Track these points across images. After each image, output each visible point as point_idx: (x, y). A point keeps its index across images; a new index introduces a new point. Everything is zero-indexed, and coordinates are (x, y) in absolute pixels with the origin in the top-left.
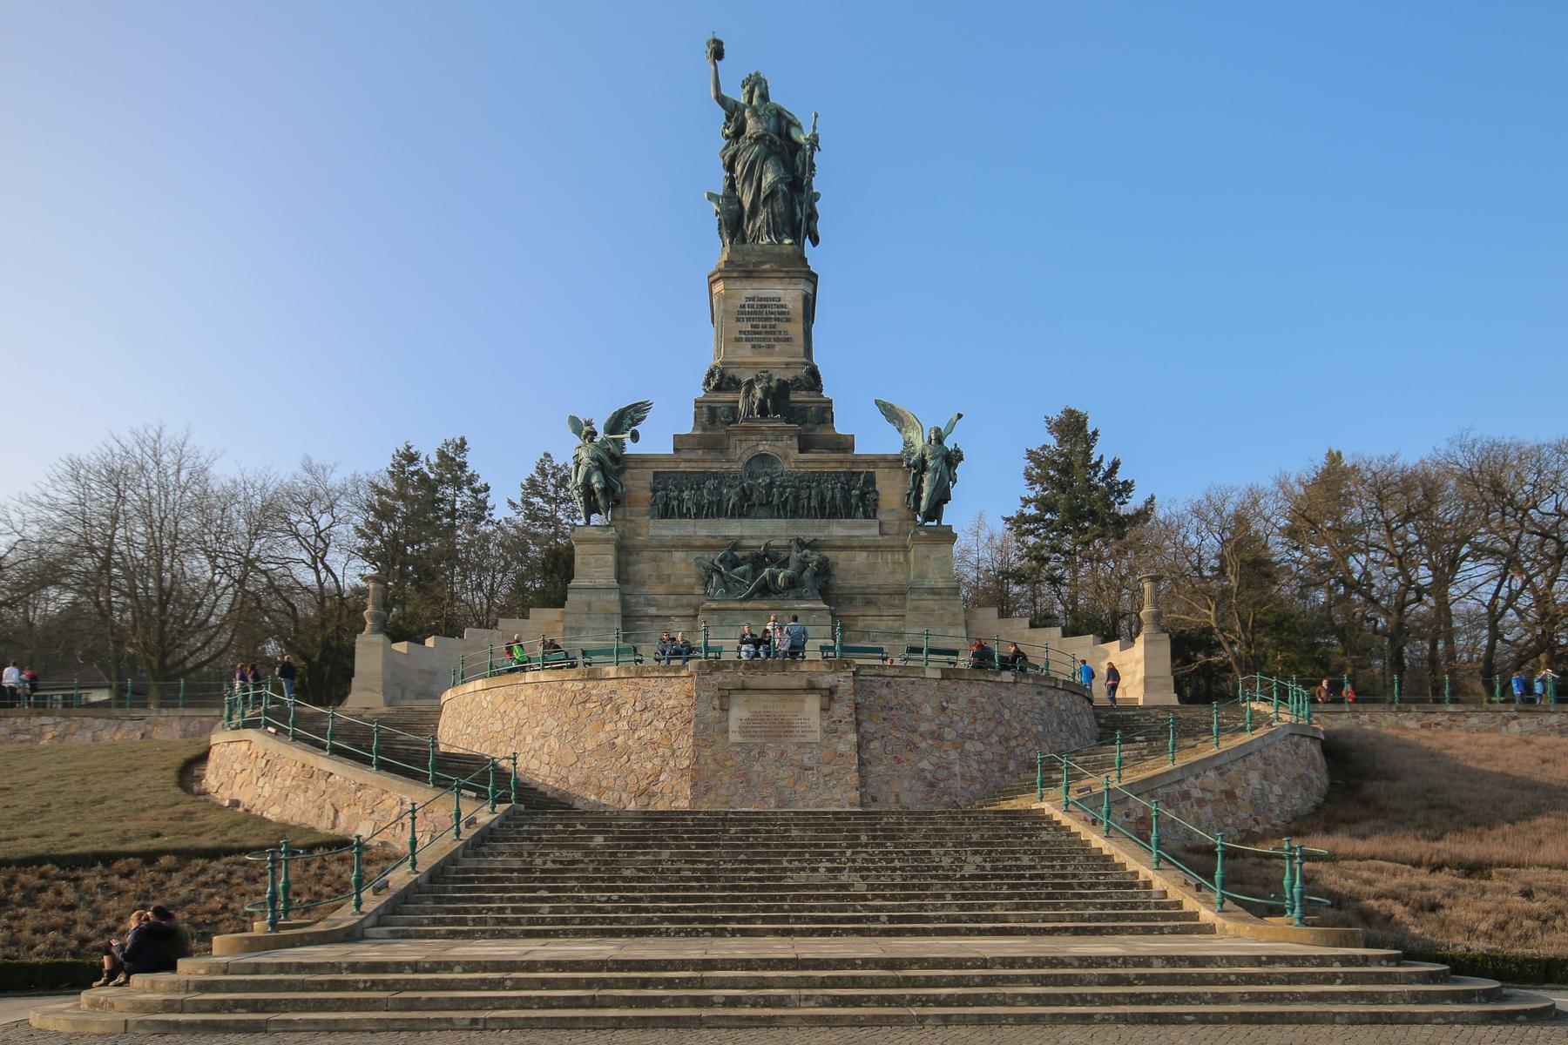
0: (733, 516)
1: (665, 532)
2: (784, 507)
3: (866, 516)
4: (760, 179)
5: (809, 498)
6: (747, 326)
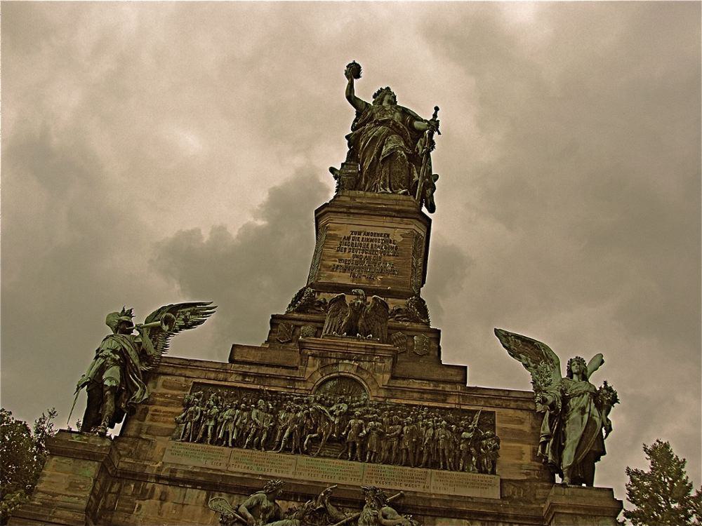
0: (286, 450)
1: (184, 461)
2: (363, 446)
3: (481, 469)
4: (381, 149)
5: (399, 437)
6: (348, 256)
